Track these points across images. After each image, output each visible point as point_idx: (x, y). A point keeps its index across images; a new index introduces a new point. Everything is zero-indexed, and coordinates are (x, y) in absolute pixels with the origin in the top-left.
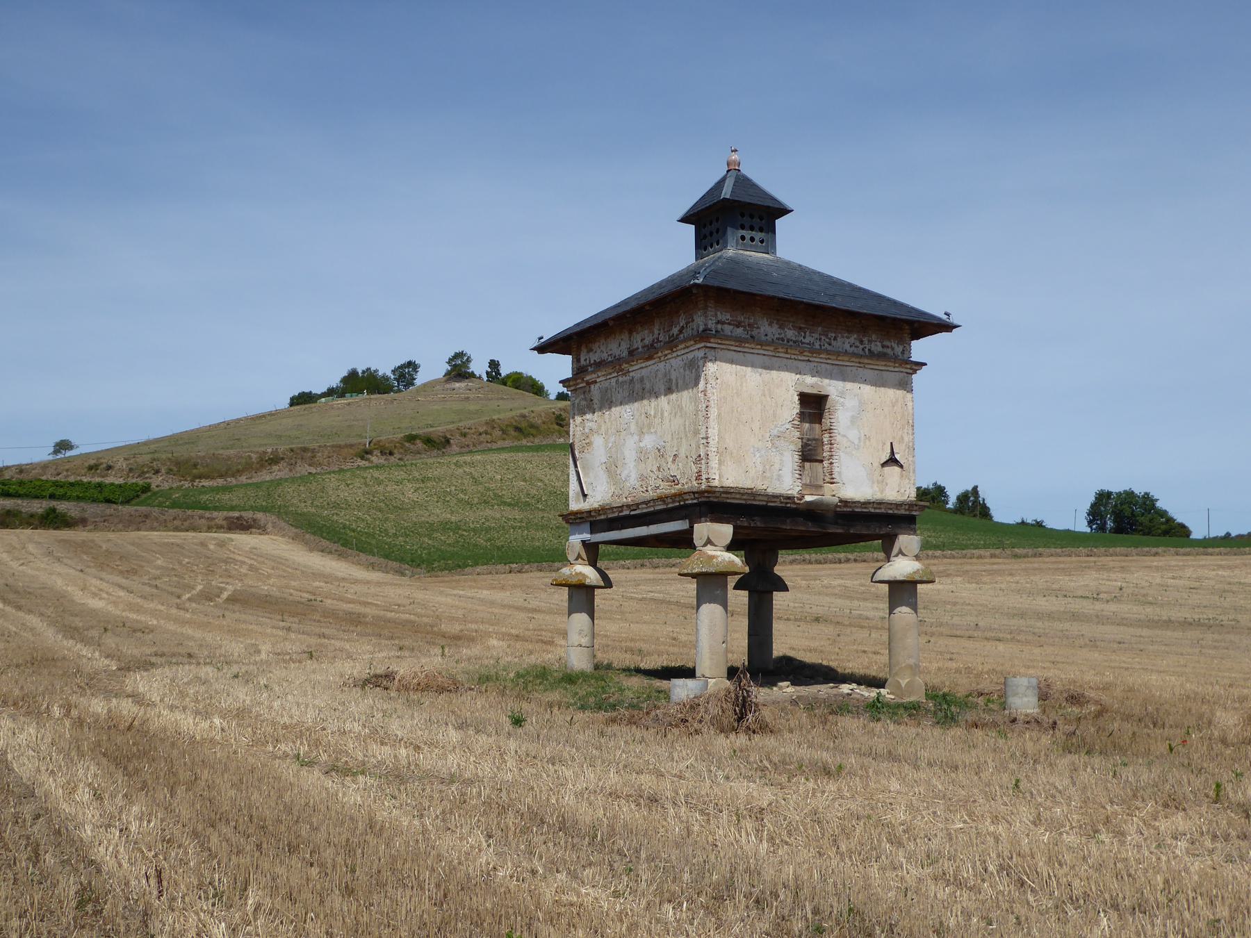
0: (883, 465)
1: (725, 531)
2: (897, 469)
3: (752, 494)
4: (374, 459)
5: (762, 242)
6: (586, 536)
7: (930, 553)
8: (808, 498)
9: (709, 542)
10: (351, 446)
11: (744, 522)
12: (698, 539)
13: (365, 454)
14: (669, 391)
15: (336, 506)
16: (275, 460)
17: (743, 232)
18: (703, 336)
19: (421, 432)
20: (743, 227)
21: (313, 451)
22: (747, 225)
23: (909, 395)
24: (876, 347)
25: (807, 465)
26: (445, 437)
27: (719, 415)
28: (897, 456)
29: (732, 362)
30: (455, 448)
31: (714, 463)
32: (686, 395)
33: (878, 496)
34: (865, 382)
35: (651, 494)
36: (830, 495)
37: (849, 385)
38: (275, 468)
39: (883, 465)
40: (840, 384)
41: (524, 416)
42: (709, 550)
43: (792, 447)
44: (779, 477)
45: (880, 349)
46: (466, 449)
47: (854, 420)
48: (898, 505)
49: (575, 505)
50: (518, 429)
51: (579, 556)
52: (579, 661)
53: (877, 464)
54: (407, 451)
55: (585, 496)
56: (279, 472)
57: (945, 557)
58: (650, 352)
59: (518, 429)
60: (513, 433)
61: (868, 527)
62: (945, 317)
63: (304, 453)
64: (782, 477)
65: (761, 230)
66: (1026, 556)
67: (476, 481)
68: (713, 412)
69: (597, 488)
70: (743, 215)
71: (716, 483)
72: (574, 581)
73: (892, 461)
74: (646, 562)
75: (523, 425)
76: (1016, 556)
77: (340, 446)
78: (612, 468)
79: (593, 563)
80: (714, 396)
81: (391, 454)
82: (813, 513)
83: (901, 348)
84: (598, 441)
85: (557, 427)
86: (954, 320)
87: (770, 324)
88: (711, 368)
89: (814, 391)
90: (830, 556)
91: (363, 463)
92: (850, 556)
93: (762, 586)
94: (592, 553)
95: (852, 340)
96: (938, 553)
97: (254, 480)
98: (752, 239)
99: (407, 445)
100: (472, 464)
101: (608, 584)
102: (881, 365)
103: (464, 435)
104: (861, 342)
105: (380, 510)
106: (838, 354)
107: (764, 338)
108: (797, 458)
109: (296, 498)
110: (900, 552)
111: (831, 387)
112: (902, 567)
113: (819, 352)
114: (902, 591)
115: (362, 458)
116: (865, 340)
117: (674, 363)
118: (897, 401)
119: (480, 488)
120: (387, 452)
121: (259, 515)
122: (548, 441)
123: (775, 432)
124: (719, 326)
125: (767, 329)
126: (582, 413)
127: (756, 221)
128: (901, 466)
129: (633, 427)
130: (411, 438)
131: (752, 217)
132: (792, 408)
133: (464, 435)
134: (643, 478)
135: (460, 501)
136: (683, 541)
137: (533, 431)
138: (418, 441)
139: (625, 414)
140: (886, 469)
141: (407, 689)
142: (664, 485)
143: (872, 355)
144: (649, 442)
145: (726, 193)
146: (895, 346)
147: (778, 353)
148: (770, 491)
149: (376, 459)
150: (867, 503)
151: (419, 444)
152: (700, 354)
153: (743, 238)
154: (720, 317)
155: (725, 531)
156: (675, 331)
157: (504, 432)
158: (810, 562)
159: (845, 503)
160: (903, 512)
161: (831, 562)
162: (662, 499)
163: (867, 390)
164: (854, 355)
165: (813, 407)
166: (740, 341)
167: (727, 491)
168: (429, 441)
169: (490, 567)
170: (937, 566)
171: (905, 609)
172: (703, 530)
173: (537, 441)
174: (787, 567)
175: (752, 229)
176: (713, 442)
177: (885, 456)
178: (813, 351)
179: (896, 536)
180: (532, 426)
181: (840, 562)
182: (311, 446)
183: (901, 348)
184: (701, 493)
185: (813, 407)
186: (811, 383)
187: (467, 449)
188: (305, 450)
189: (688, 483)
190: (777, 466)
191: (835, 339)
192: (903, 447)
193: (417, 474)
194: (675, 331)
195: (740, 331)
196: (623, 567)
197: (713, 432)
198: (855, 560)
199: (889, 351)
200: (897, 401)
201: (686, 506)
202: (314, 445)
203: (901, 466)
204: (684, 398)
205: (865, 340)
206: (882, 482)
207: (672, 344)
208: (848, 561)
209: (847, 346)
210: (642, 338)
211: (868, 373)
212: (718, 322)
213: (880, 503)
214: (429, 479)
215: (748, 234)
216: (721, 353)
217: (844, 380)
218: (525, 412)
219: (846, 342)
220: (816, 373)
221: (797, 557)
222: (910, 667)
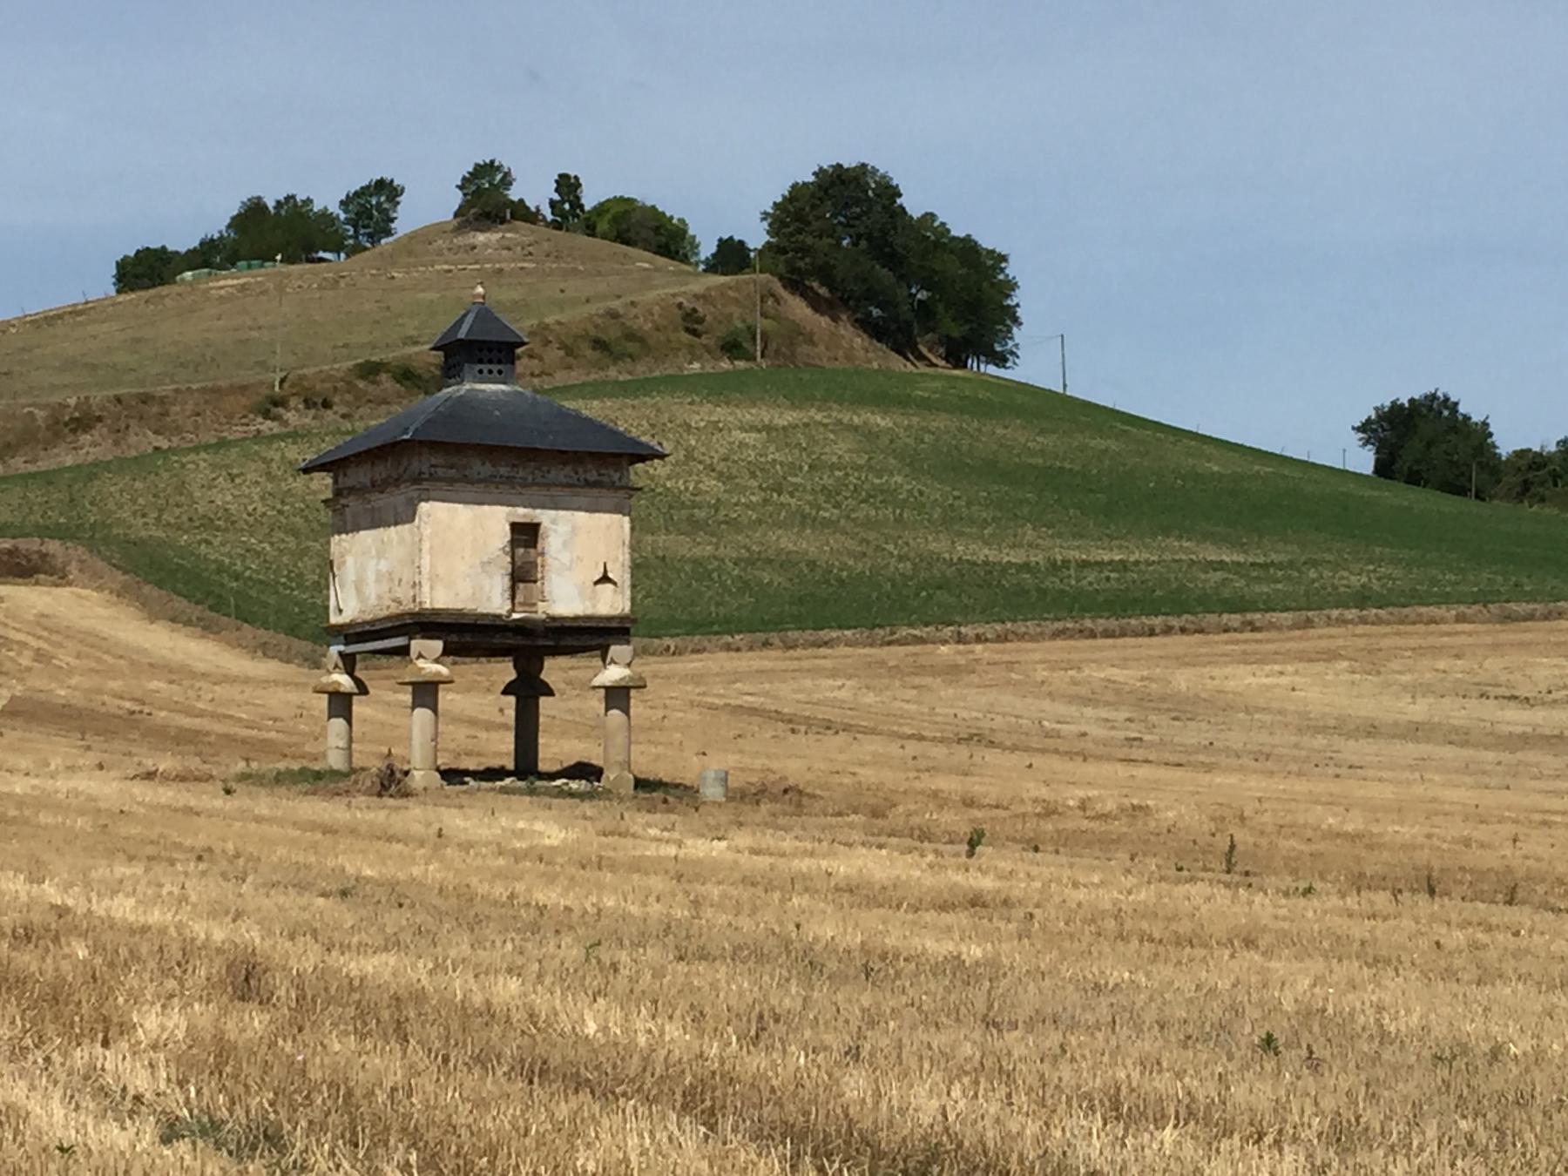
0: (596, 583)
1: (438, 645)
2: (610, 586)
3: (460, 613)
4: (290, 416)
5: (500, 372)
6: (342, 648)
7: (1335, 613)
8: (515, 616)
9: (420, 656)
10: (243, 389)
11: (454, 638)
12: (413, 654)
13: (271, 406)
14: (396, 524)
15: (208, 523)
16: (83, 422)
17: (480, 366)
18: (417, 480)
20: (481, 361)
21: (162, 400)
24: (593, 476)
25: (521, 585)
27: (431, 548)
29: (444, 501)
31: (426, 588)
32: (407, 526)
33: (589, 612)
34: (579, 509)
35: (385, 613)
36: (543, 610)
37: (562, 513)
38: (86, 438)
39: (596, 583)
40: (553, 513)
41: (614, 315)
42: (421, 663)
44: (489, 599)
47: (565, 543)
48: (609, 619)
49: (334, 619)
50: (599, 344)
51: (336, 666)
52: (336, 761)
55: (341, 611)
56: (92, 447)
57: (1363, 621)
58: (379, 486)
59: (599, 344)
60: (589, 352)
61: (589, 637)
63: (144, 407)
64: (493, 599)
65: (499, 362)
66: (1530, 617)
68: (426, 546)
69: (350, 602)
71: (427, 606)
72: (330, 689)
73: (605, 579)
74: (775, 638)
75: (613, 334)
76: (1508, 618)
77: (217, 391)
78: (359, 586)
79: (351, 673)
80: (427, 531)
81: (327, 405)
84: (350, 560)
85: (686, 337)
88: (424, 507)
91: (267, 426)
92: (1175, 622)
93: (528, 691)
94: (349, 664)
96: (1352, 614)
97: (43, 465)
98: (490, 372)
99: (361, 384)
101: (363, 689)
102: (595, 491)
105: (294, 532)
106: (548, 486)
108: (507, 581)
110: (613, 662)
111: (544, 517)
112: (613, 674)
114: (617, 696)
115: (267, 415)
116: (580, 470)
117: (393, 499)
121: (53, 546)
122: (669, 369)
125: (481, 468)
126: (340, 533)
128: (615, 584)
129: (374, 552)
130: (370, 370)
131: (490, 350)
132: (503, 535)
134: (379, 597)
136: (404, 651)
137: (632, 347)
138: (383, 377)
139: (366, 537)
140: (599, 586)
141: (167, 779)
142: (393, 605)
143: (589, 484)
144: (384, 566)
145: (462, 334)
146: (611, 472)
148: (479, 610)
150: (576, 618)
151: (386, 382)
152: (415, 494)
154: (434, 461)
155: (438, 645)
156: (401, 470)
157: (569, 351)
158: (1092, 635)
159: (553, 619)
161: (1137, 635)
162: (388, 618)
163: (581, 516)
165: (525, 535)
166: (451, 481)
167: (436, 612)
171: (615, 712)
172: (417, 645)
173: (641, 369)
174: (554, 670)
175: (490, 362)
176: (425, 571)
178: (524, 486)
180: (631, 336)
181: (1152, 633)
182: (160, 391)
184: (418, 614)
185: (525, 535)
186: (522, 514)
188: (145, 399)
189: (409, 606)
192: (618, 565)
194: (401, 470)
196: (728, 648)
197: (426, 562)
198: (1183, 630)
199: (605, 479)
201: (406, 625)
202: (166, 389)
203: (615, 584)
204: (404, 529)
205: (580, 470)
206: (594, 598)
207: (397, 482)
208: (1168, 631)
210: (381, 471)
211: (583, 500)
216: (433, 494)
217: (556, 508)
218: (616, 304)
219: (560, 473)
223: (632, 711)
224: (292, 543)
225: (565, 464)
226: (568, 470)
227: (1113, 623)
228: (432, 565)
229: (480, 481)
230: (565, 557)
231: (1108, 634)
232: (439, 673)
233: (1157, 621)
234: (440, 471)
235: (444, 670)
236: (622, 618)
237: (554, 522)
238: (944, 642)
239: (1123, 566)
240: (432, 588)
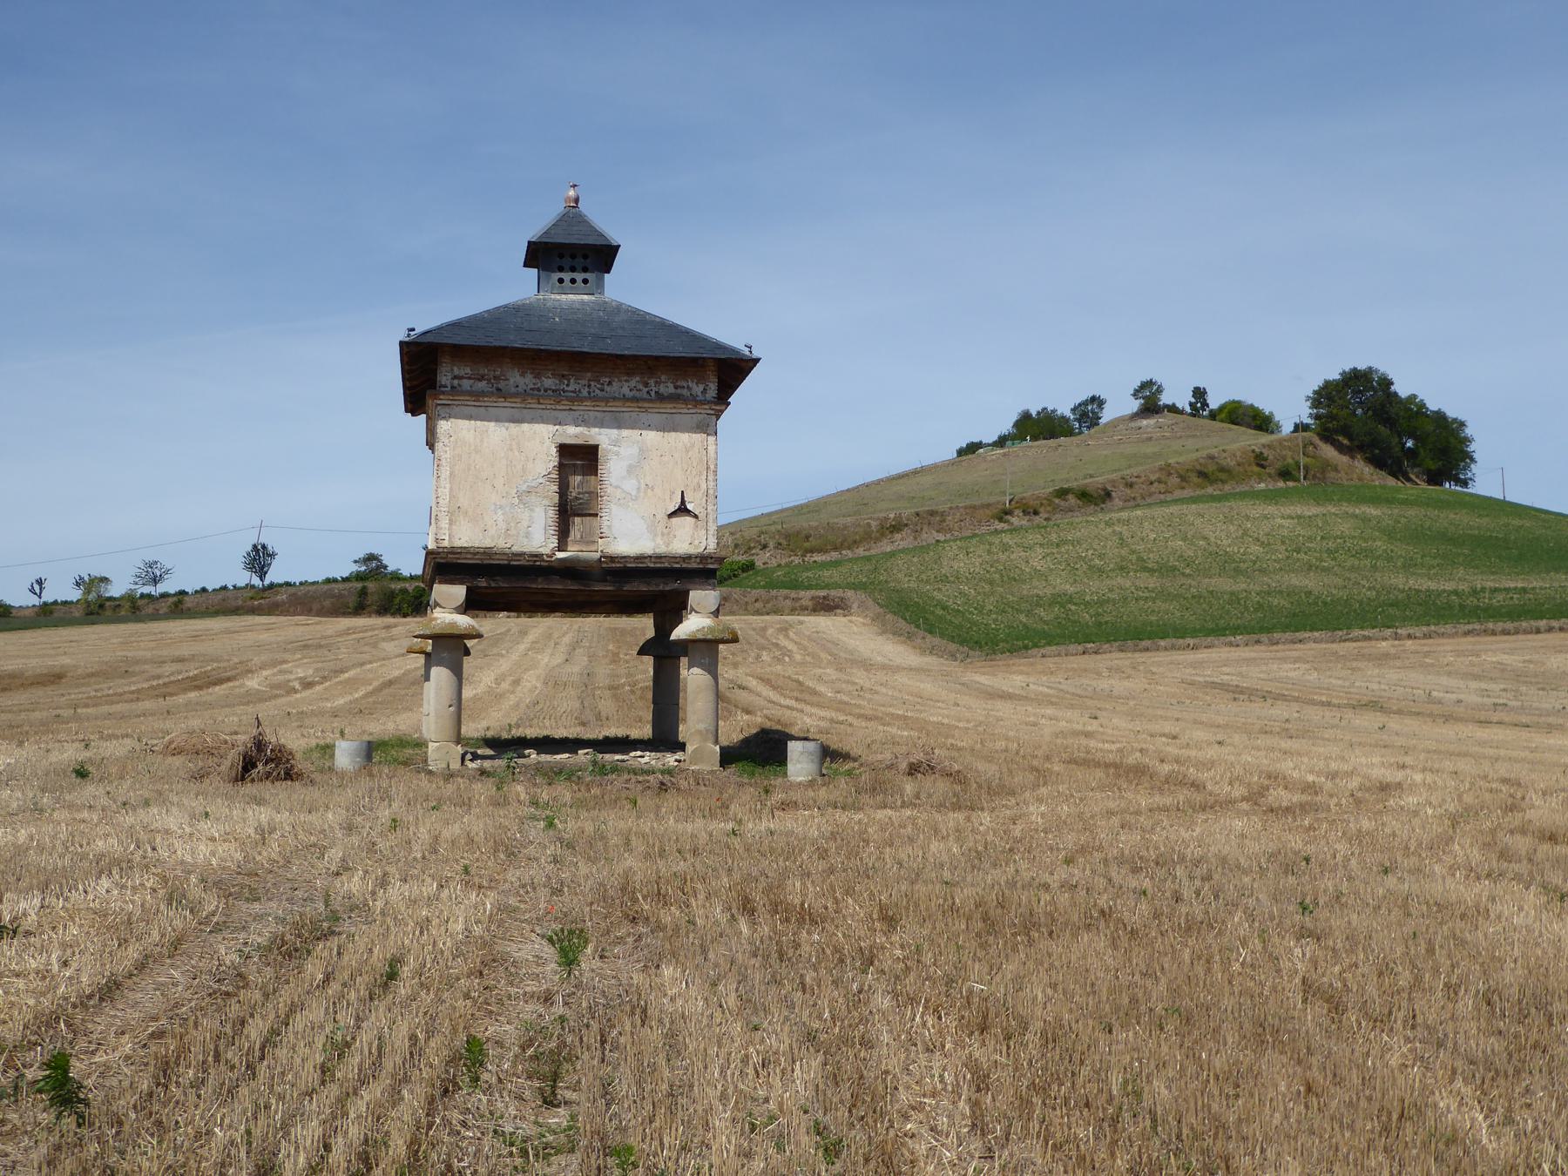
0: (671, 515)
1: (459, 592)
2: (689, 519)
3: (488, 552)
4: (1014, 520)
5: (585, 281)
10: (988, 506)
13: (1002, 516)
15: (944, 579)
16: (896, 527)
17: (562, 275)
19: (1074, 485)
20: (561, 269)
21: (942, 514)
22: (567, 267)
23: (711, 439)
26: (1105, 489)
28: (690, 507)
29: (470, 418)
30: (1117, 502)
33: (662, 549)
34: (649, 427)
37: (625, 433)
38: (898, 536)
39: (671, 515)
41: (1211, 457)
43: (546, 502)
44: (527, 535)
45: (671, 389)
46: (1132, 503)
47: (631, 470)
48: (688, 558)
50: (1202, 474)
53: (662, 515)
54: (1056, 509)
56: (902, 540)
59: (1202, 474)
60: (1196, 480)
62: (746, 351)
63: (932, 518)
64: (534, 534)
65: (585, 270)
67: (1122, 542)
70: (561, 256)
71: (446, 544)
73: (683, 510)
74: (1264, 638)
75: (1211, 468)
77: (974, 507)
81: (1036, 513)
82: (571, 571)
83: (701, 387)
85: (1256, 469)
86: (756, 354)
87: (523, 375)
89: (579, 442)
90: (1524, 624)
91: (1000, 526)
92: (1555, 624)
95: (633, 383)
97: (873, 552)
98: (573, 281)
99: (1057, 501)
100: (1128, 522)
103: (1131, 485)
104: (646, 385)
105: (991, 583)
106: (606, 400)
107: (513, 390)
108: (552, 513)
109: (904, 576)
113: (582, 400)
115: (1001, 520)
116: (652, 382)
118: (693, 445)
119: (1124, 552)
120: (1031, 511)
121: (850, 593)
122: (1243, 488)
123: (524, 488)
124: (456, 382)
125: (517, 379)
127: (579, 262)
128: (696, 516)
130: (1062, 493)
131: (573, 257)
132: (550, 459)
133: (1131, 485)
135: (1091, 567)
137: (1223, 476)
138: (1070, 497)
140: (674, 520)
143: (661, 398)
147: (527, 405)
148: (515, 549)
149: (1016, 520)
151: (1072, 499)
153: (561, 281)
154: (456, 371)
155: (459, 592)
157: (1183, 478)
158: (1494, 633)
159: (612, 559)
160: (695, 566)
161: (1526, 632)
163: (651, 436)
164: (635, 399)
165: (579, 460)
166: (477, 395)
168: (1084, 496)
169: (1062, 648)
170: (736, 622)
173: (1227, 487)
175: (573, 270)
177: (674, 505)
178: (572, 400)
179: (687, 593)
180: (1222, 469)
181: (1538, 631)
182: (941, 508)
183: (701, 387)
185: (579, 460)
186: (573, 433)
187: (1132, 503)
188: (932, 513)
190: (525, 524)
191: (610, 383)
192: (700, 494)
193: (1054, 537)
195: (482, 385)
196: (1231, 644)
199: (685, 392)
200: (693, 445)
202: (945, 507)
203: (696, 516)
205: (652, 382)
208: (1550, 630)
209: (625, 390)
211: (655, 418)
212: (455, 377)
213: (659, 557)
214: (1065, 542)
215: (567, 276)
216: (457, 409)
217: (619, 427)
218: (1214, 452)
219: (624, 387)
220: (585, 422)
221: (1477, 626)
222: (700, 732)
223: (722, 669)
224: (987, 588)
225: (630, 373)
226: (634, 381)
227: (1509, 625)
228: (452, 497)
229: (516, 395)
230: (630, 485)
231: (1505, 632)
232: (453, 625)
233: (1543, 623)
234: (466, 384)
235: (464, 621)
236: (703, 558)
237: (616, 443)
238: (1385, 639)
239: (1524, 590)
240: (451, 523)
